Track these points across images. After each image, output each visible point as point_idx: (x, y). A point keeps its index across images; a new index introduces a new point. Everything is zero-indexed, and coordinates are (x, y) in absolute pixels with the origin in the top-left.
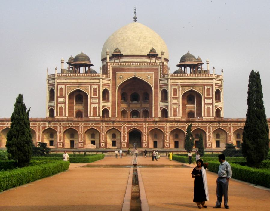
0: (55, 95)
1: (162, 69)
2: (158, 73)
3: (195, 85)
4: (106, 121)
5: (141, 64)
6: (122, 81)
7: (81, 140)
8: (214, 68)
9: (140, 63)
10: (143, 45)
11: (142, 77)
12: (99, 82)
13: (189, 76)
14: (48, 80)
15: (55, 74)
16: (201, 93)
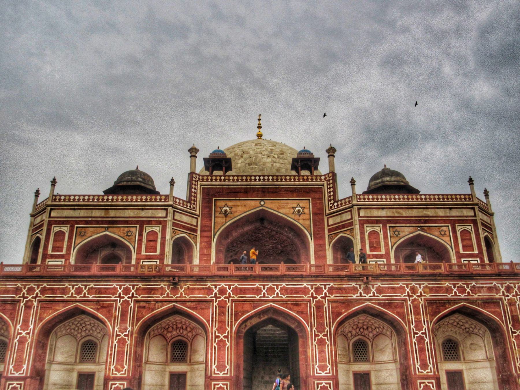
0: (41, 250)
1: (332, 189)
2: (321, 199)
3: (426, 222)
4: (144, 278)
5: (277, 180)
6: (228, 219)
7: (18, 368)
8: (471, 181)
9: (275, 178)
10: (278, 165)
11: (280, 211)
12: (165, 216)
13: (408, 199)
14: (33, 218)
15: (48, 198)
16: (446, 244)
